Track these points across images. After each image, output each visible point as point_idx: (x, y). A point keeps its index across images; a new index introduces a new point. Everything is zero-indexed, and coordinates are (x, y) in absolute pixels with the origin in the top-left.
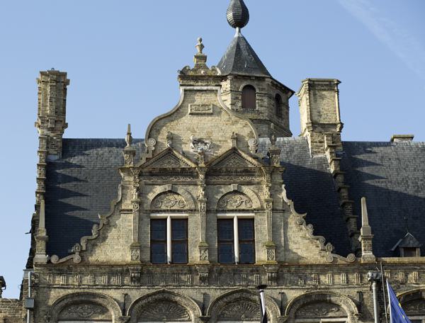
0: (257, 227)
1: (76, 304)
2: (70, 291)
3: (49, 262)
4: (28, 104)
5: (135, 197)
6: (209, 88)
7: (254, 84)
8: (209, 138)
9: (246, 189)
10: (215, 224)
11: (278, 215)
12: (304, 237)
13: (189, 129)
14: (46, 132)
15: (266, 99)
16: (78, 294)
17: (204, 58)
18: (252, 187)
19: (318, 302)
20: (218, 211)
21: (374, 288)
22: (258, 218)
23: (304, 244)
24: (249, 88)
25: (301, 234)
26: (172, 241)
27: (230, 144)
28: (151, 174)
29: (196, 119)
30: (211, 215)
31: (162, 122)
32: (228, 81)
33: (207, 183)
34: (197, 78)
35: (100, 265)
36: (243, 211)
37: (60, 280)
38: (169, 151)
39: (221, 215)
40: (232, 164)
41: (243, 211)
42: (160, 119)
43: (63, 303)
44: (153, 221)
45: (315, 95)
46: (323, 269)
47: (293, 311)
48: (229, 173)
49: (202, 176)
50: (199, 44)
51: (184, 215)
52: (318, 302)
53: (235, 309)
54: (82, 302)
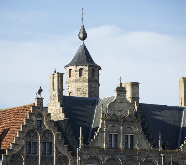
7: (94, 68)
10: (124, 137)
12: (146, 142)
13: (118, 107)
18: (133, 126)
19: (149, 161)
20: (125, 133)
21: (163, 159)
23: (146, 145)
24: (93, 69)
25: (145, 141)
29: (120, 104)
31: (111, 105)
32: (87, 67)
34: (121, 91)
35: (97, 147)
44: (109, 134)
45: (133, 88)
46: (151, 151)
50: (120, 79)
52: (149, 161)
53: (129, 162)
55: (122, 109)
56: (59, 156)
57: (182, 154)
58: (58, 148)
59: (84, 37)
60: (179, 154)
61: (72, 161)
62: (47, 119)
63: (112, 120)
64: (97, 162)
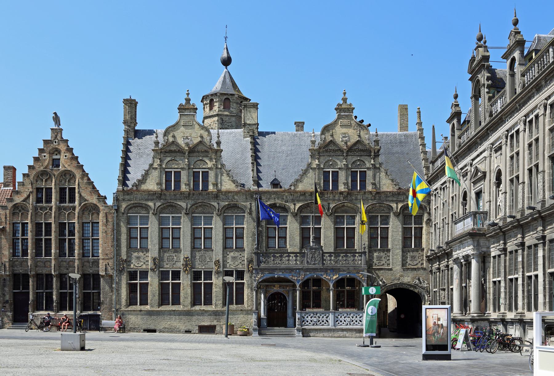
0: (210, 175)
1: (135, 207)
2: (132, 202)
3: (123, 190)
4: (120, 112)
5: (159, 163)
6: (191, 113)
7: (230, 97)
8: (191, 136)
9: (205, 159)
10: (192, 174)
11: (218, 170)
14: (127, 127)
15: (235, 104)
16: (136, 203)
17: (190, 100)
19: (234, 207)
20: (193, 168)
22: (210, 172)
26: (175, 181)
27: (199, 139)
28: (166, 152)
30: (190, 170)
31: (170, 129)
33: (189, 156)
34: (185, 109)
36: (204, 168)
37: (127, 197)
38: (173, 142)
39: (194, 170)
40: (200, 148)
41: (204, 168)
42: (169, 127)
43: (129, 207)
47: (223, 210)
48: (198, 152)
49: (187, 153)
51: (179, 170)
52: (234, 207)
54: (137, 206)
55: (188, 135)
56: (84, 205)
57: (292, 194)
58: (82, 194)
59: (227, 62)
60: (286, 194)
61: (105, 211)
62: (66, 156)
63: (171, 152)
64: (146, 210)
